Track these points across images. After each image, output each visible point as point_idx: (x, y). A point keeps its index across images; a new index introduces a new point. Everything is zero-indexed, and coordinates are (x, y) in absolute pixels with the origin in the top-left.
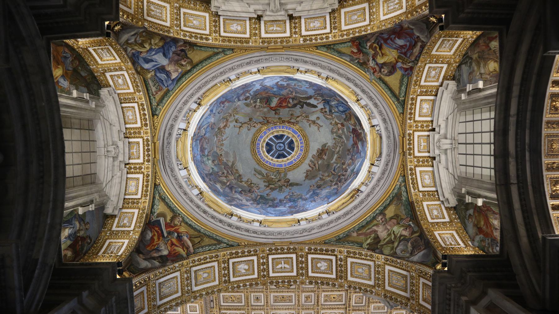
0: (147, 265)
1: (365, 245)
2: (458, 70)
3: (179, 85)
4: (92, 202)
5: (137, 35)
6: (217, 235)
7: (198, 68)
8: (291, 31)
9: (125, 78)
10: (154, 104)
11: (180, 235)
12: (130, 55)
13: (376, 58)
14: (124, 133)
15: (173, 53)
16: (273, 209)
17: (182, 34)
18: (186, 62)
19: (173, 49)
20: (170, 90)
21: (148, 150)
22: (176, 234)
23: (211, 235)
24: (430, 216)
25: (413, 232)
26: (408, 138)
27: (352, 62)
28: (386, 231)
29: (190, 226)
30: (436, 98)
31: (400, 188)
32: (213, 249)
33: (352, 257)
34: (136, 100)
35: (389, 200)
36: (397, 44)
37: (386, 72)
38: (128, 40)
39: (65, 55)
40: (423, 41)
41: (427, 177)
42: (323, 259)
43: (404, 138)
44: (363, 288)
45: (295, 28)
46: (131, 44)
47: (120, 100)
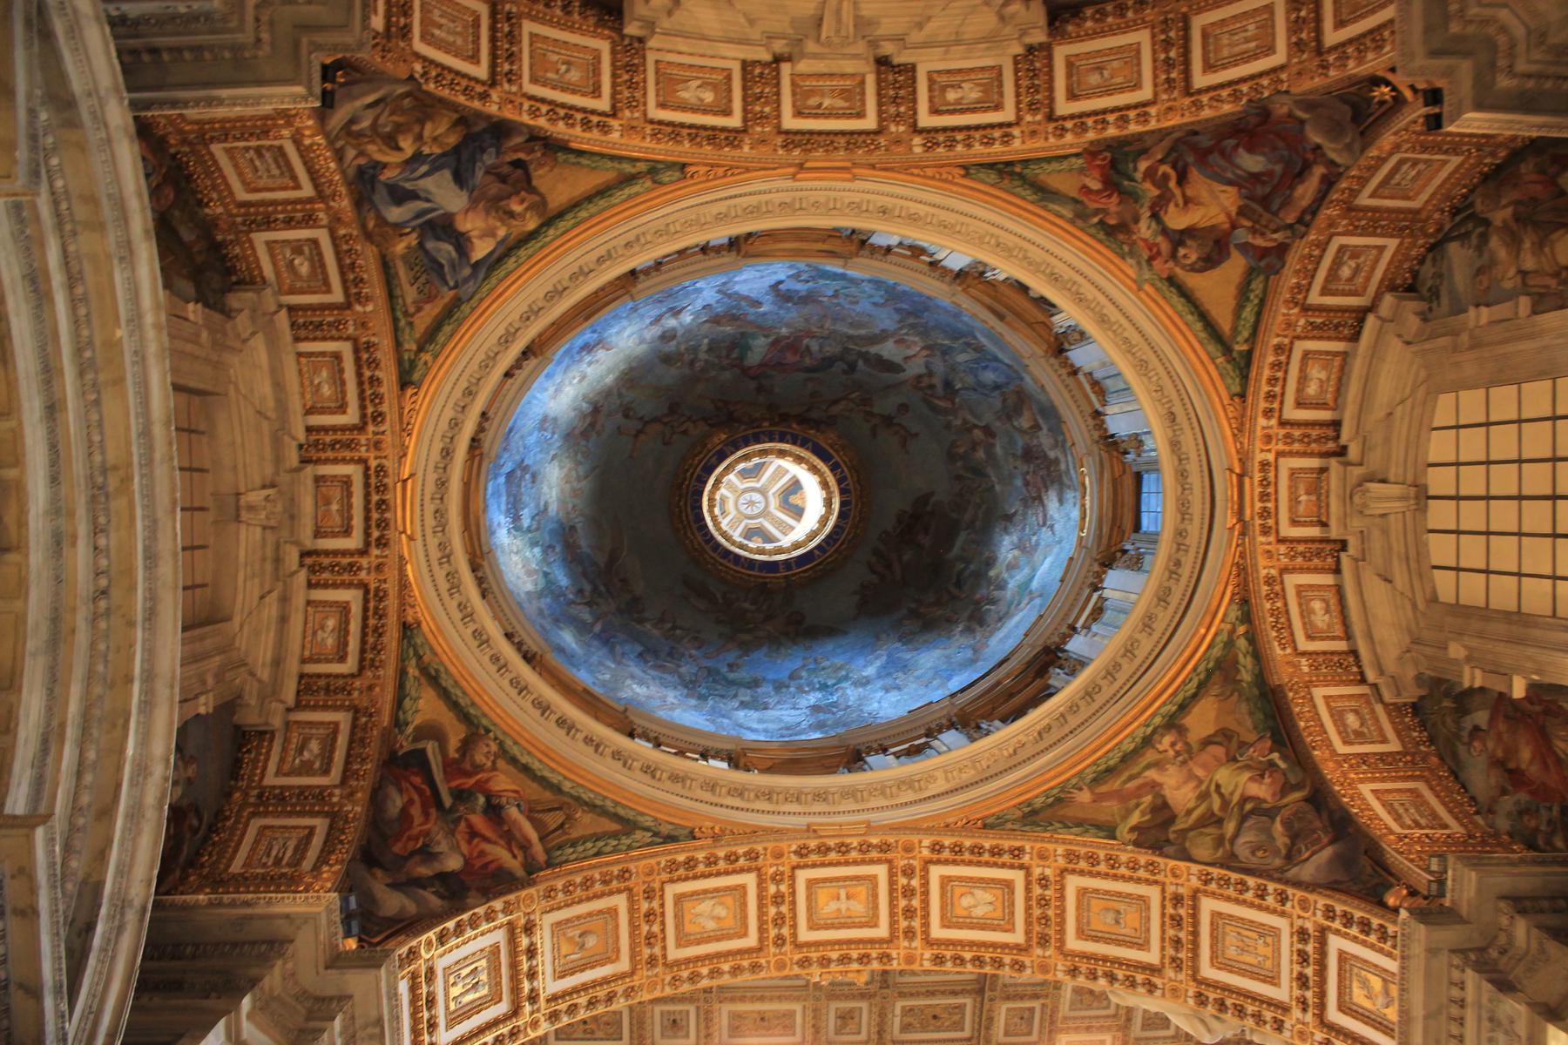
0: (403, 908)
1: (1123, 831)
3: (494, 281)
6: (617, 803)
7: (562, 225)
8: (880, 113)
9: (320, 254)
10: (407, 346)
11: (495, 801)
12: (351, 172)
14: (301, 447)
15: (487, 172)
16: (754, 715)
17: (526, 107)
19: (489, 159)
20: (464, 298)
22: (482, 800)
23: (598, 802)
25: (1286, 789)
26: (1257, 476)
27: (1079, 223)
28: (1192, 784)
29: (526, 769)
30: (1356, 349)
31: (1230, 643)
32: (608, 849)
33: (1082, 873)
35: (1195, 682)
36: (1239, 167)
37: (1193, 257)
38: (353, 121)
40: (1333, 163)
42: (982, 880)
43: (1247, 480)
46: (360, 134)
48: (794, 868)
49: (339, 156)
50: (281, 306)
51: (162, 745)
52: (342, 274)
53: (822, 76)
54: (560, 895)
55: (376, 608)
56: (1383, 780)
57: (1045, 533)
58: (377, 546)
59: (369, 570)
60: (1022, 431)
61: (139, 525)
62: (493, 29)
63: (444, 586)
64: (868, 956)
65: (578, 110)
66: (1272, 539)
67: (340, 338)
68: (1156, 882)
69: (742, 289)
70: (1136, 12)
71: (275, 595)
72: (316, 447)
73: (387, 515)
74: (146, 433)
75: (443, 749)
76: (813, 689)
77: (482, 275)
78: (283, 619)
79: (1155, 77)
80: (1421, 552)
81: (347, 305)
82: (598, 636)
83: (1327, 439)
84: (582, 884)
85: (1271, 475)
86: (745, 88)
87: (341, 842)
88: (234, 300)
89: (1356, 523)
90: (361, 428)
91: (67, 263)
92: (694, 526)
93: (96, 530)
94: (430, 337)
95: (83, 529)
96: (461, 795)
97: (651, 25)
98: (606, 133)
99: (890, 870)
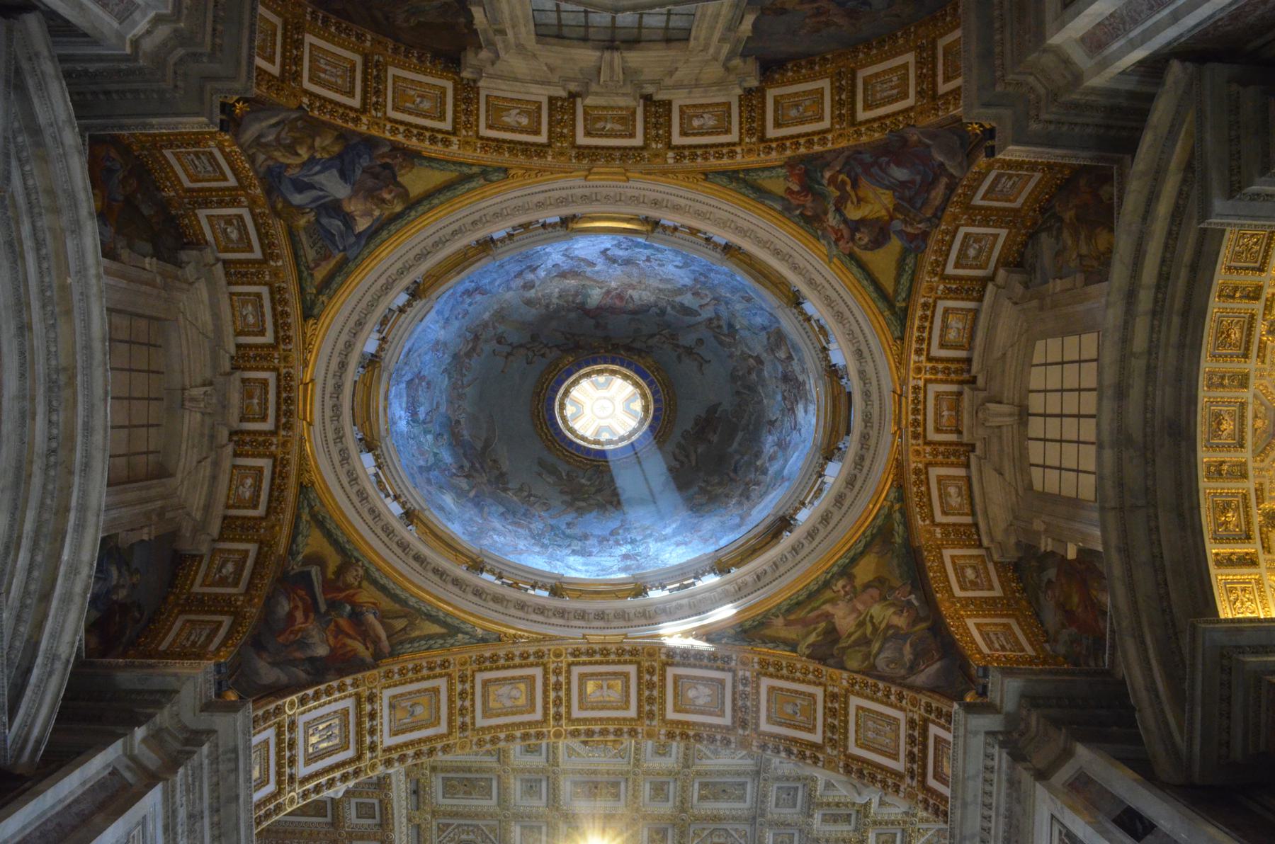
1: (803, 648)
3: (372, 246)
5: (282, 125)
7: (420, 209)
8: (646, 134)
9: (245, 226)
11: (358, 610)
12: (262, 170)
14: (232, 358)
15: (363, 171)
16: (579, 559)
17: (388, 126)
18: (393, 194)
19: (365, 162)
22: (348, 608)
23: (434, 613)
24: (959, 582)
25: (915, 621)
26: (911, 397)
27: (787, 214)
28: (854, 615)
29: (383, 589)
31: (889, 516)
32: (437, 646)
33: (771, 676)
34: (267, 278)
35: (862, 544)
37: (866, 240)
38: (260, 136)
39: (109, 164)
40: (951, 176)
43: (904, 399)
44: (795, 752)
46: (266, 145)
49: (252, 159)
50: (218, 260)
51: (89, 553)
52: (260, 240)
53: (604, 108)
54: (396, 676)
55: (281, 471)
56: (984, 616)
57: (795, 434)
58: (284, 429)
59: (277, 446)
60: (780, 360)
61: (80, 408)
62: (365, 73)
63: (336, 458)
64: (620, 730)
65: (426, 128)
66: (920, 441)
67: (260, 284)
68: (820, 684)
70: (821, 66)
71: (209, 460)
72: (244, 358)
73: (292, 407)
74: (88, 347)
75: (323, 572)
76: (626, 543)
77: (363, 242)
78: (214, 478)
79: (832, 112)
80: (1024, 453)
81: (264, 261)
82: (472, 500)
83: (962, 371)
84: (412, 669)
85: (921, 396)
86: (550, 116)
87: (238, 632)
88: (184, 255)
89: (981, 432)
90: (274, 347)
91: (35, 234)
92: (549, 423)
93: (51, 409)
95: (41, 409)
96: (333, 605)
97: (480, 71)
98: (447, 146)
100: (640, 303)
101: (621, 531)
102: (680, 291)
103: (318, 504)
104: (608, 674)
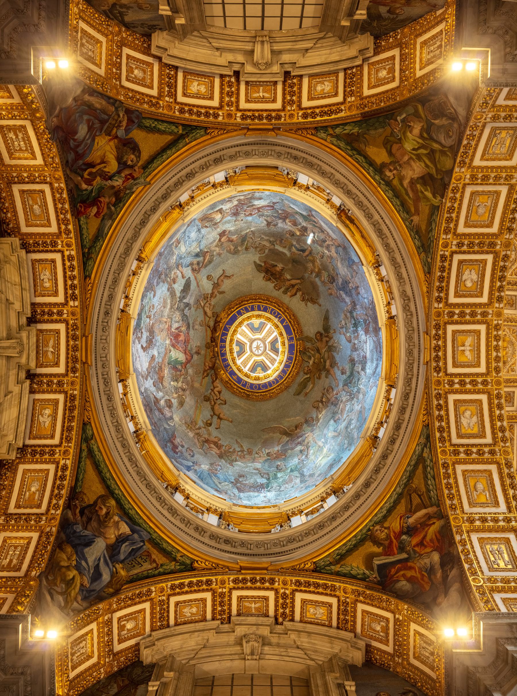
2: (134, 27)
3: (141, 521)
4: (341, 686)
5: (52, 591)
6: (409, 464)
7: (113, 486)
8: (56, 321)
9: (125, 616)
11: (405, 530)
12: (85, 604)
13: (109, 174)
14: (222, 623)
15: (86, 529)
16: (369, 364)
17: (53, 512)
18: (103, 507)
19: (79, 528)
20: (149, 537)
21: (253, 581)
22: (404, 537)
23: (408, 474)
24: (388, 83)
26: (249, 121)
27: (114, 216)
29: (390, 511)
30: (182, 68)
32: (432, 472)
33: (456, 225)
34: (164, 598)
37: (133, 156)
41: (319, 88)
42: (457, 276)
43: (250, 127)
45: (51, 314)
47: (161, 627)
48: (447, 375)
64: (495, 336)
66: (283, 114)
69: (146, 365)
73: (258, 578)
75: (378, 555)
90: (214, 592)
94: (167, 554)
99: (450, 324)
100: (181, 322)
101: (348, 335)
102: (172, 293)
103: (328, 559)
104: (453, 347)
